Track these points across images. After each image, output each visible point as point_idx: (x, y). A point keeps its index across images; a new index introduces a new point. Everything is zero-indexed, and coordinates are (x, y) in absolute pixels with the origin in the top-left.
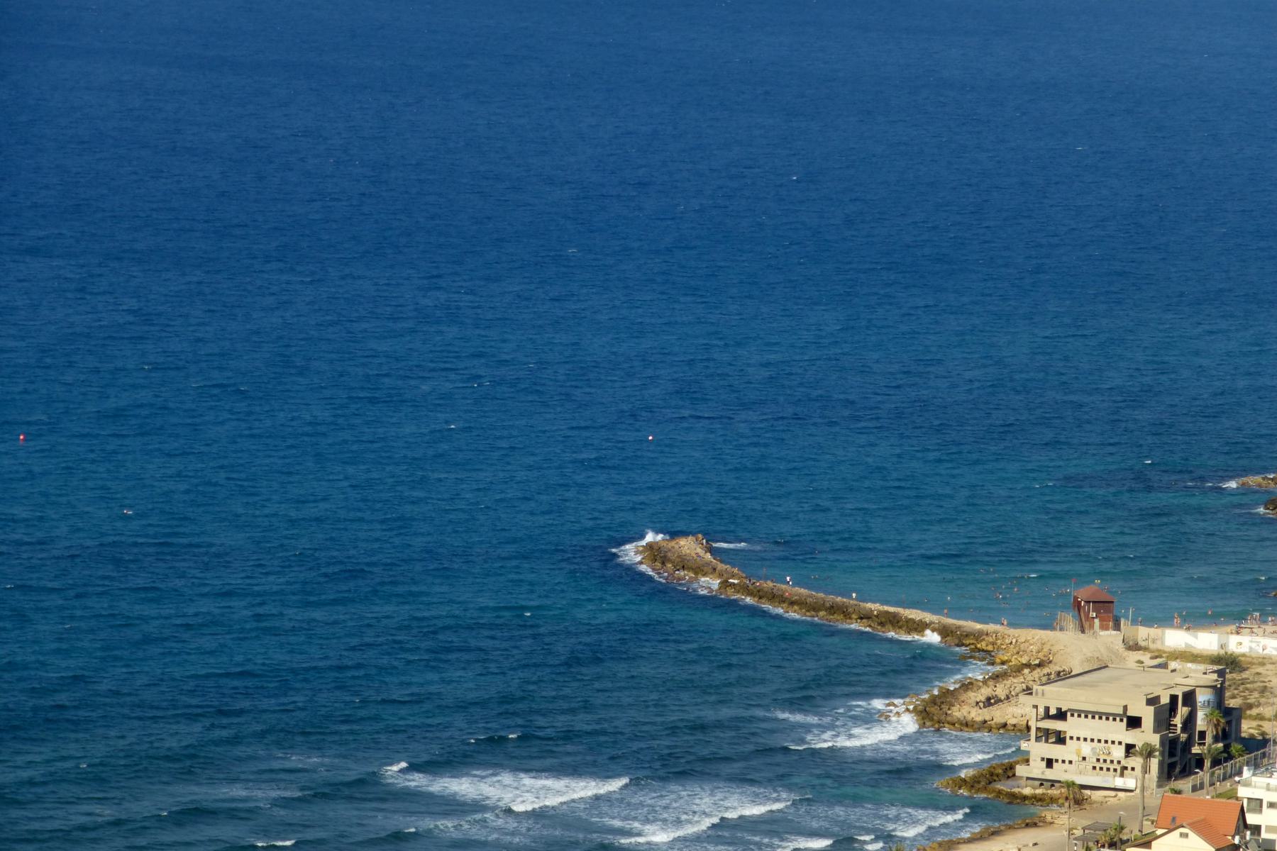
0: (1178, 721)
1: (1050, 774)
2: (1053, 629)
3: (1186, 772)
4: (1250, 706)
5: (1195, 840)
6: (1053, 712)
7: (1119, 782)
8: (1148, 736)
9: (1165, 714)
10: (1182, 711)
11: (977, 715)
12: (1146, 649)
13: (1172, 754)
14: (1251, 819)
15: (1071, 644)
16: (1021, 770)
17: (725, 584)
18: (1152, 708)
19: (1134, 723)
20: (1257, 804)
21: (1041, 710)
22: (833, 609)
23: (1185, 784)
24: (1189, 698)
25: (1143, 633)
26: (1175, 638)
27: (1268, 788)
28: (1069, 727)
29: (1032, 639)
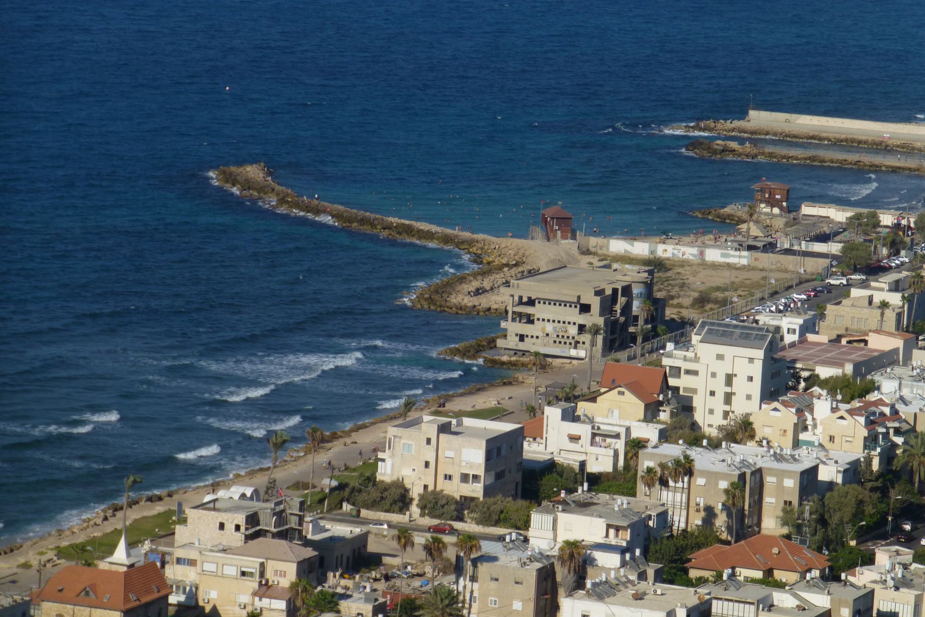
0: (618, 308)
1: (522, 346)
2: (526, 238)
3: (623, 346)
4: (672, 298)
5: (629, 397)
6: (525, 299)
7: (573, 352)
8: (595, 318)
9: (608, 304)
10: (622, 300)
11: (468, 301)
12: (595, 254)
13: (613, 332)
14: (672, 382)
15: (539, 249)
16: (500, 343)
17: (282, 201)
18: (598, 298)
19: (585, 309)
20: (676, 371)
21: (516, 298)
22: (363, 221)
23: (623, 355)
24: (627, 290)
25: (593, 241)
26: (617, 246)
27: (685, 359)
28: (537, 311)
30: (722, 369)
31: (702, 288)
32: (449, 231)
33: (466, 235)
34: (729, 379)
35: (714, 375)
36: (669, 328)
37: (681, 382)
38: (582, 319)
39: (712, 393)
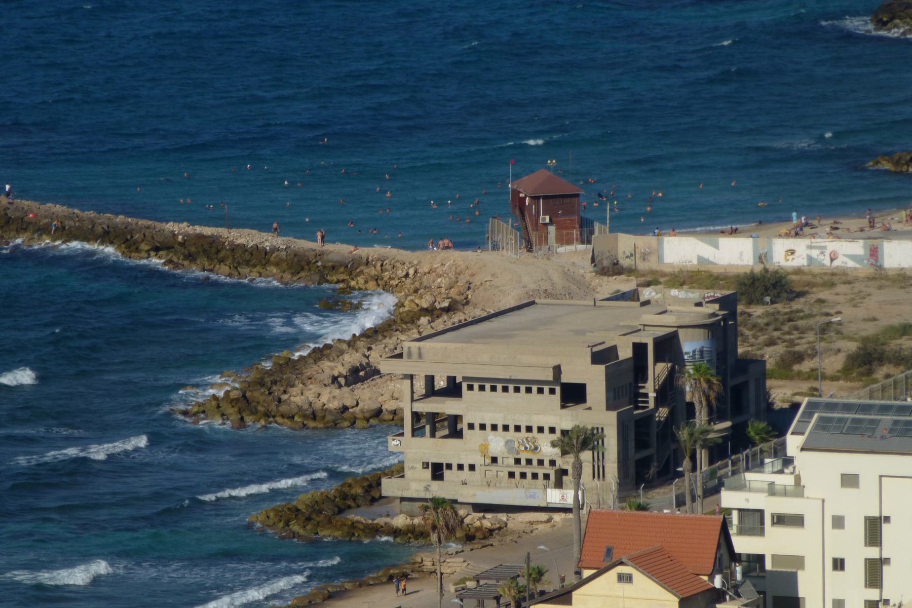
0: (650, 389)
1: (438, 490)
4: (799, 358)
7: (554, 497)
9: (625, 378)
10: (657, 371)
12: (631, 271)
13: (641, 444)
15: (501, 269)
16: (389, 487)
18: (601, 369)
19: (574, 394)
20: (753, 521)
26: (681, 250)
27: (772, 490)
28: (470, 407)
29: (440, 265)
30: (857, 507)
31: (870, 330)
32: (303, 244)
33: (340, 250)
34: (874, 529)
35: (838, 522)
36: (749, 423)
37: (770, 544)
38: (570, 419)
39: (839, 564)
